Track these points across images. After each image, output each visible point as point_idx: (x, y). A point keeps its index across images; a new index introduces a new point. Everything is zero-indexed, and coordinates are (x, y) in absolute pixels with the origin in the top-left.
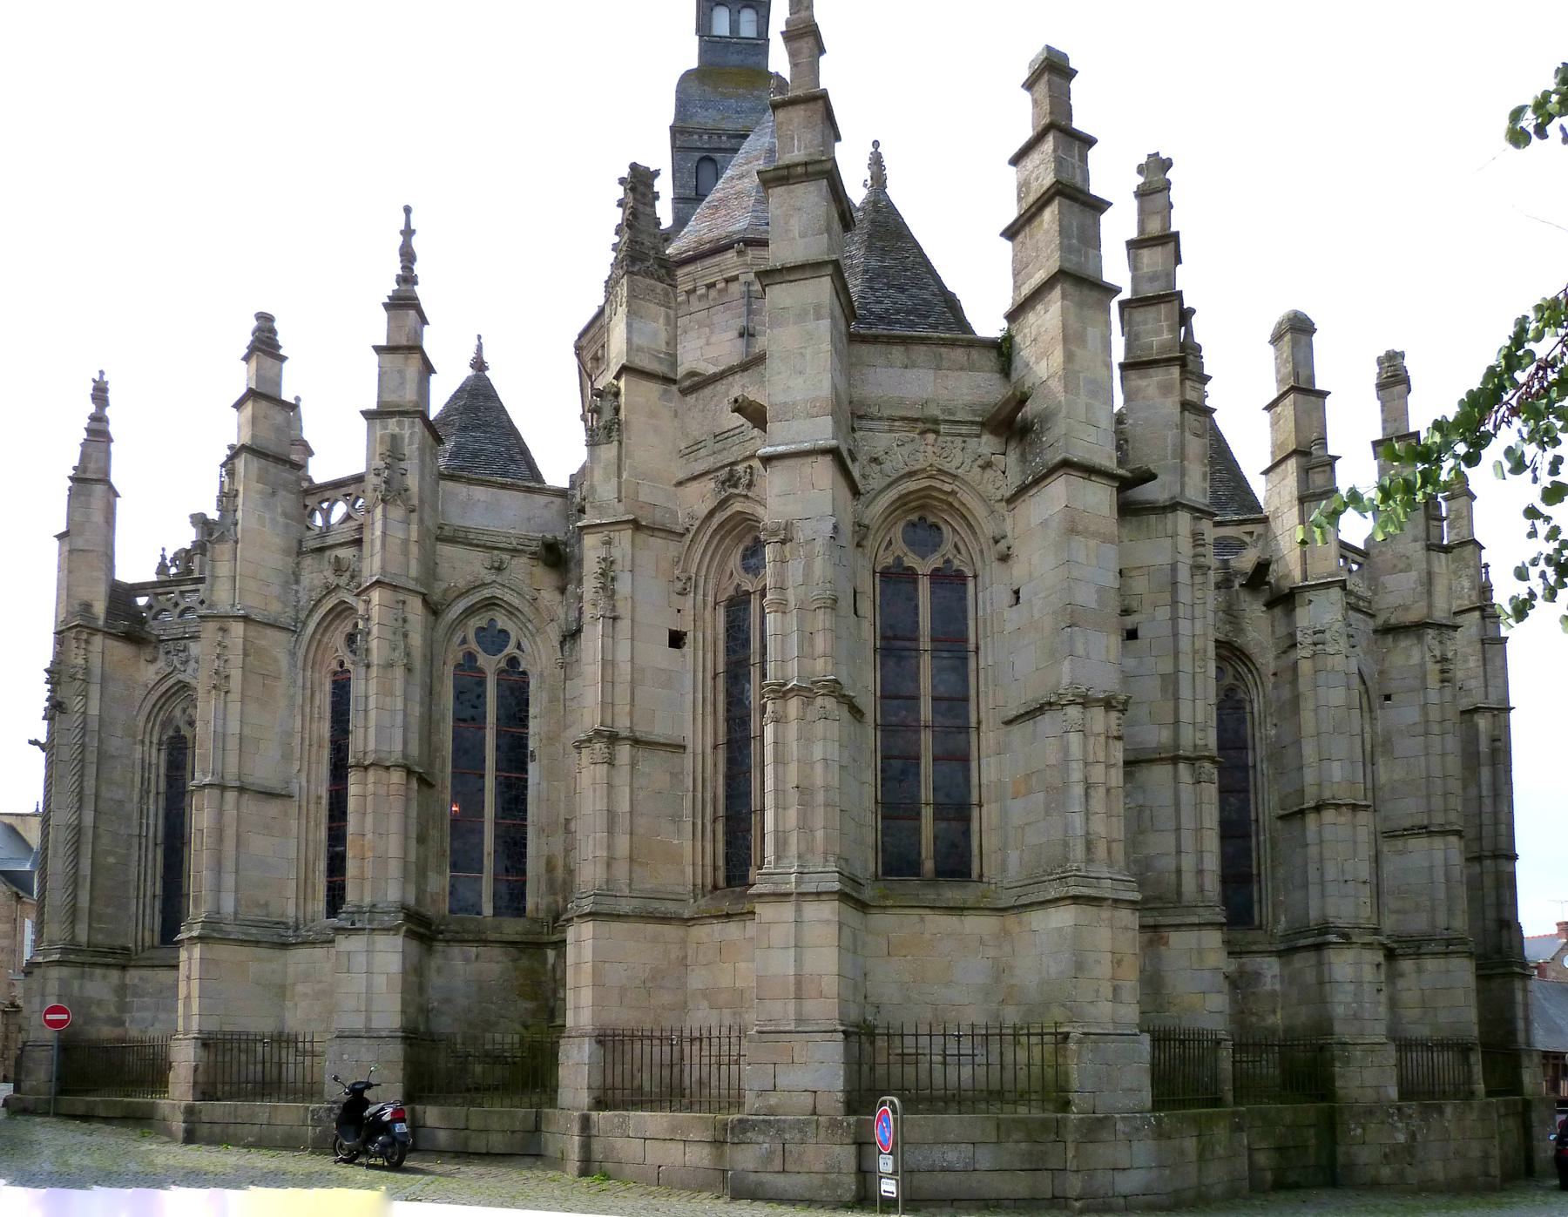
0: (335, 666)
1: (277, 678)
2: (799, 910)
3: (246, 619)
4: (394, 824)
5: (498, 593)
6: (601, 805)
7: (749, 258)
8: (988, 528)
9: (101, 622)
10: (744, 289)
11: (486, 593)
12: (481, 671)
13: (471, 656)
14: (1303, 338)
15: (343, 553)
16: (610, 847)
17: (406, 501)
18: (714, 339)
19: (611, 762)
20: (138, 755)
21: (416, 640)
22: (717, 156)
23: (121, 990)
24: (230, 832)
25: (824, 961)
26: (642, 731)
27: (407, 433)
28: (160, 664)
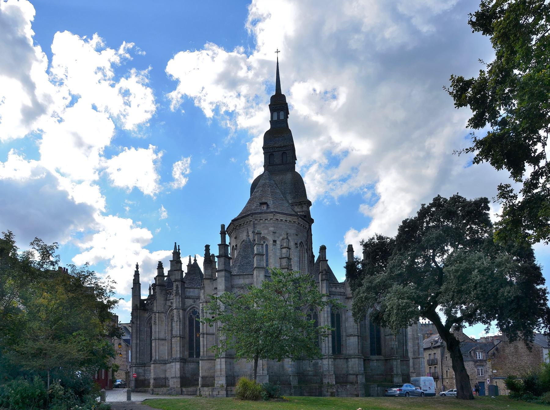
1: (163, 321)
2: (221, 360)
4: (178, 345)
5: (195, 306)
11: (193, 306)
14: (324, 250)
15: (172, 301)
17: (179, 295)
21: (181, 316)
23: (144, 370)
24: (157, 346)
25: (224, 366)
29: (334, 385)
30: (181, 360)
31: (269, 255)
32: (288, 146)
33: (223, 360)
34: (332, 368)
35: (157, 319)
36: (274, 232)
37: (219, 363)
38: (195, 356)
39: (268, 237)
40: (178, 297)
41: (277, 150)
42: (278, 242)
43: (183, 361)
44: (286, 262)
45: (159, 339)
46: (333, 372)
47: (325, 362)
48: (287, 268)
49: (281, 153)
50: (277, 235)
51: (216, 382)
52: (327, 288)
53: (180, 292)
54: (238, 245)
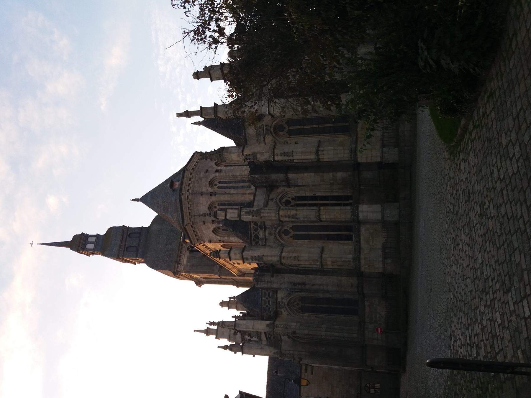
3: (281, 253)
5: (278, 199)
7: (184, 193)
9: (272, 322)
10: (191, 195)
22: (126, 246)
27: (245, 210)
28: (282, 310)
32: (124, 231)
39: (211, 178)
41: (124, 244)
42: (219, 168)
50: (210, 169)
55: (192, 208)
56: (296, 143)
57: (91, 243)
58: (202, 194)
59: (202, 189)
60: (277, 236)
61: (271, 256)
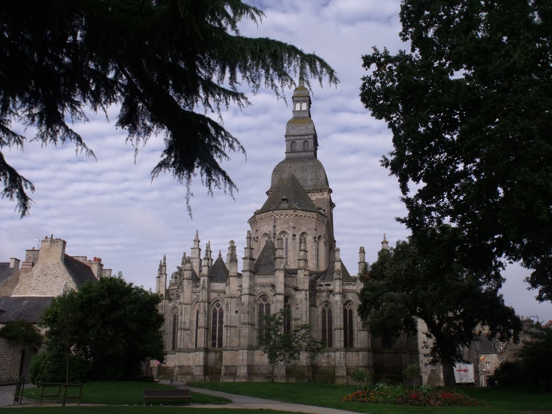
0: (197, 309)
5: (219, 299)
6: (226, 335)
7: (274, 213)
8: (271, 299)
11: (217, 299)
12: (217, 310)
13: (215, 308)
15: (198, 293)
16: (227, 341)
18: (269, 227)
19: (227, 330)
20: (169, 318)
21: (206, 309)
22: (296, 141)
25: (245, 357)
26: (231, 325)
28: (173, 303)
29: (344, 376)
30: (205, 349)
31: (289, 248)
33: (245, 351)
34: (343, 361)
35: (183, 311)
36: (294, 227)
37: (241, 354)
38: (217, 347)
39: (288, 232)
40: (204, 291)
42: (298, 237)
43: (207, 351)
44: (304, 264)
45: (184, 330)
46: (344, 364)
47: (338, 354)
48: (305, 269)
49: (303, 141)
51: (238, 372)
52: (340, 286)
53: (206, 286)
54: (260, 238)
55: (266, 220)
56: (237, 312)
57: (301, 107)
58: (274, 227)
59: (278, 226)
60: (196, 301)
61: (183, 298)
